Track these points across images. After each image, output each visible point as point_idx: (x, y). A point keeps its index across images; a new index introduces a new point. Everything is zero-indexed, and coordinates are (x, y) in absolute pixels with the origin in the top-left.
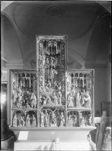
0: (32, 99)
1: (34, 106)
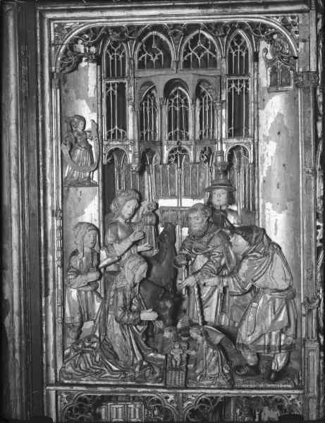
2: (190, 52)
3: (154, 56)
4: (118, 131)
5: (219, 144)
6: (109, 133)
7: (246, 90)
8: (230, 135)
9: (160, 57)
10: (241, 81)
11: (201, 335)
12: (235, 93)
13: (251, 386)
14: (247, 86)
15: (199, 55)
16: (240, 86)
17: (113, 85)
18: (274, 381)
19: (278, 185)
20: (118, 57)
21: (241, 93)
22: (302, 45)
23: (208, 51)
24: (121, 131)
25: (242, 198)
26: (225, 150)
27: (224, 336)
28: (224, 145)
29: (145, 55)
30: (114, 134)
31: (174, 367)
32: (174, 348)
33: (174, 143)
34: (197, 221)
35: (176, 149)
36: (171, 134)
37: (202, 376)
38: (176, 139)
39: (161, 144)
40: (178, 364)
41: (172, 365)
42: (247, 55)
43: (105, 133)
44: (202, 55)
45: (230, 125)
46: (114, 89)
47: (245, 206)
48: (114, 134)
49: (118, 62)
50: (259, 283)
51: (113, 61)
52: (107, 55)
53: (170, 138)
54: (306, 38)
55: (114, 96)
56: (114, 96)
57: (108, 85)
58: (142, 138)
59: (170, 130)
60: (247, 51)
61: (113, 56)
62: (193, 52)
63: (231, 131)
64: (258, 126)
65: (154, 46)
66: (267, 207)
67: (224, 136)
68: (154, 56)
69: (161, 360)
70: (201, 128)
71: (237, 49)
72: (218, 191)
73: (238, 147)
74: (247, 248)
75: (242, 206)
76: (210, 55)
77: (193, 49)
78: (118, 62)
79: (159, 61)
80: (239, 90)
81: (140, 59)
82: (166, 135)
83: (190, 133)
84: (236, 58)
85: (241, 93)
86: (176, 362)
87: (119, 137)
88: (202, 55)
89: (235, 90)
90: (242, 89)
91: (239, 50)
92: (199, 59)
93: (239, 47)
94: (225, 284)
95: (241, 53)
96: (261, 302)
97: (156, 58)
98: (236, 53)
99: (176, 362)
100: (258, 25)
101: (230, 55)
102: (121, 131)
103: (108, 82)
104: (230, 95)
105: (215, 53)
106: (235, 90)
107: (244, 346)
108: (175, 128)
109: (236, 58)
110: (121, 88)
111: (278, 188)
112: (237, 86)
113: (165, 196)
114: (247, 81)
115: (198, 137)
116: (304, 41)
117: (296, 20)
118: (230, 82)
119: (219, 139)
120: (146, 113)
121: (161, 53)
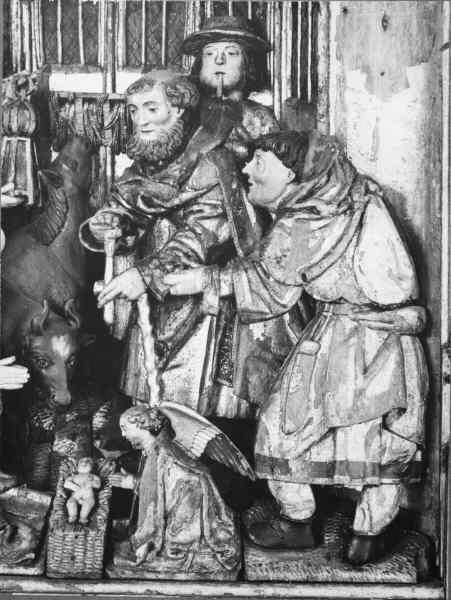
0: (309, 312)
1: (335, 502)
11: (154, 432)
13: (291, 576)
18: (356, 564)
19: (385, 22)
25: (286, 73)
27: (218, 431)
31: (71, 519)
32: (76, 473)
34: (151, 116)
37: (151, 547)
40: (85, 512)
41: (66, 514)
47: (294, 94)
50: (325, 286)
66: (349, 83)
69: (42, 506)
72: (218, 48)
74: (290, 189)
75: (287, 93)
86: (79, 507)
94: (225, 291)
96: (326, 340)
99: (79, 507)
107: (280, 465)
111: (385, 28)
113: (69, 61)
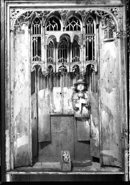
2: (69, 24)
3: (53, 26)
4: (38, 57)
5: (82, 63)
6: (34, 58)
7: (93, 40)
8: (87, 60)
9: (56, 26)
10: (91, 37)
12: (89, 42)
14: (94, 39)
15: (73, 26)
16: (91, 39)
17: (36, 38)
20: (38, 26)
21: (91, 42)
22: (119, 20)
23: (77, 24)
24: (39, 57)
26: (84, 66)
28: (84, 64)
29: (50, 25)
30: (36, 59)
33: (61, 65)
35: (61, 66)
36: (59, 60)
38: (61, 62)
39: (55, 64)
42: (93, 26)
43: (32, 58)
44: (74, 25)
45: (87, 55)
46: (36, 39)
48: (36, 59)
49: (38, 28)
51: (36, 28)
52: (33, 25)
53: (59, 62)
54: (121, 17)
55: (36, 42)
56: (36, 42)
57: (33, 38)
58: (48, 60)
59: (59, 58)
60: (93, 24)
61: (36, 26)
62: (70, 24)
63: (87, 58)
64: (99, 55)
65: (53, 22)
67: (84, 60)
68: (53, 26)
70: (73, 57)
71: (89, 23)
73: (90, 65)
76: (78, 26)
77: (70, 22)
78: (38, 28)
79: (75, 27)
80: (90, 40)
81: (48, 27)
82: (57, 60)
83: (68, 59)
84: (89, 27)
85: (91, 42)
87: (38, 60)
88: (74, 25)
89: (88, 40)
90: (92, 40)
91: (90, 24)
92: (73, 27)
93: (90, 22)
95: (91, 25)
97: (54, 26)
98: (89, 25)
100: (100, 12)
101: (86, 26)
102: (39, 57)
103: (33, 36)
104: (86, 42)
105: (80, 25)
106: (88, 40)
108: (61, 57)
109: (36, 28)
110: (39, 39)
112: (89, 39)
114: (93, 37)
115: (71, 61)
116: (120, 18)
117: (116, 10)
118: (87, 37)
119: (82, 61)
120: (49, 51)
121: (57, 25)
